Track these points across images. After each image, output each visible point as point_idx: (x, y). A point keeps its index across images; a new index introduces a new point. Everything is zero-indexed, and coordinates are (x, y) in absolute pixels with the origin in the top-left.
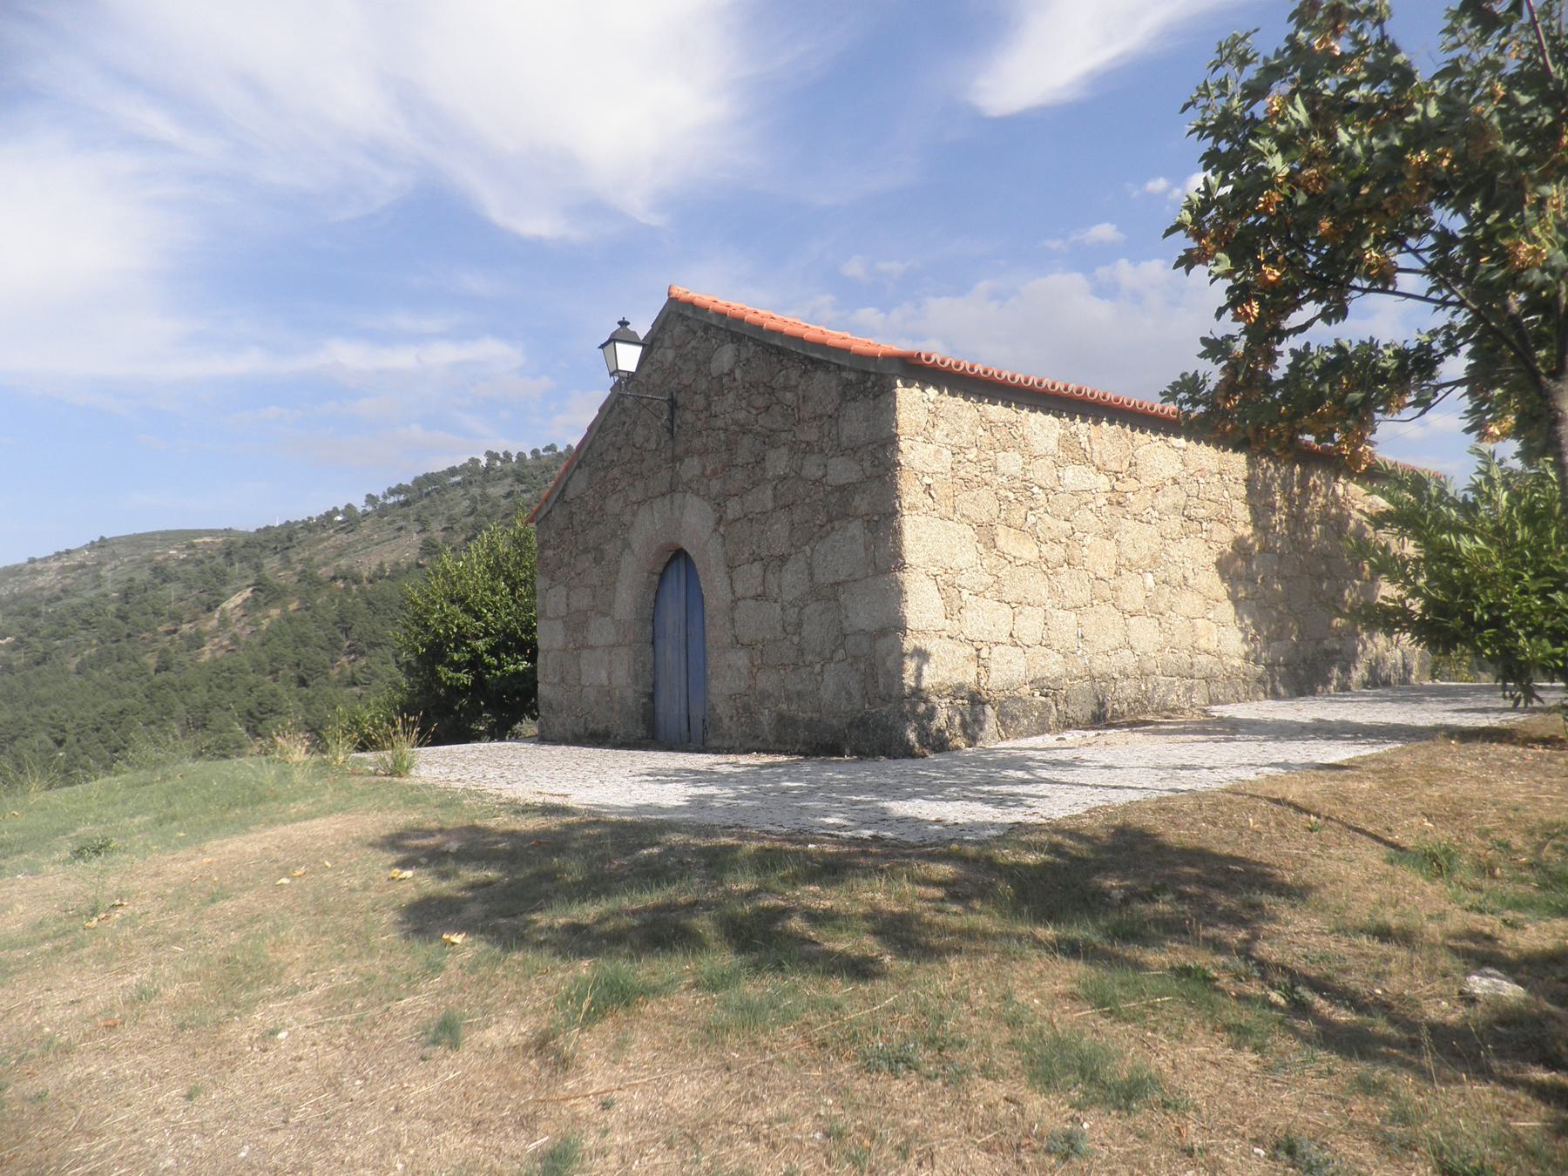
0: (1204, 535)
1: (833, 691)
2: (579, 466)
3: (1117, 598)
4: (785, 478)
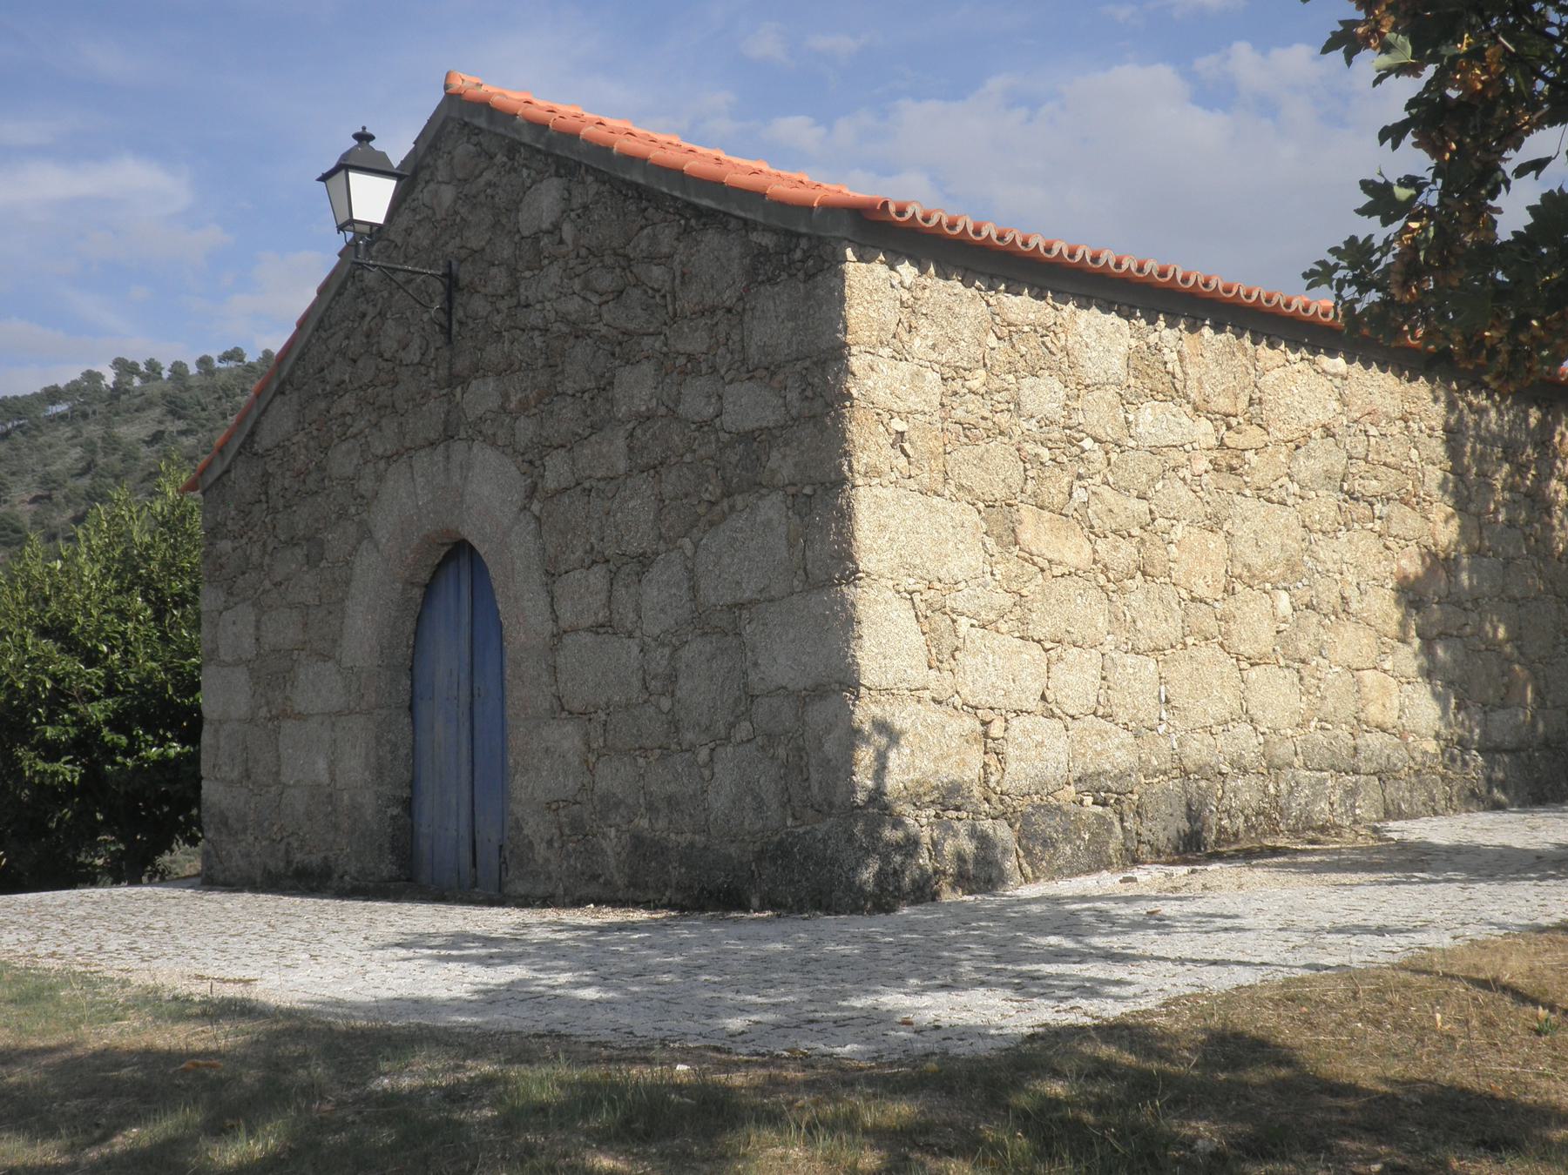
0: (1377, 525)
1: (731, 794)
2: (281, 391)
3: (1227, 634)
4: (647, 418)
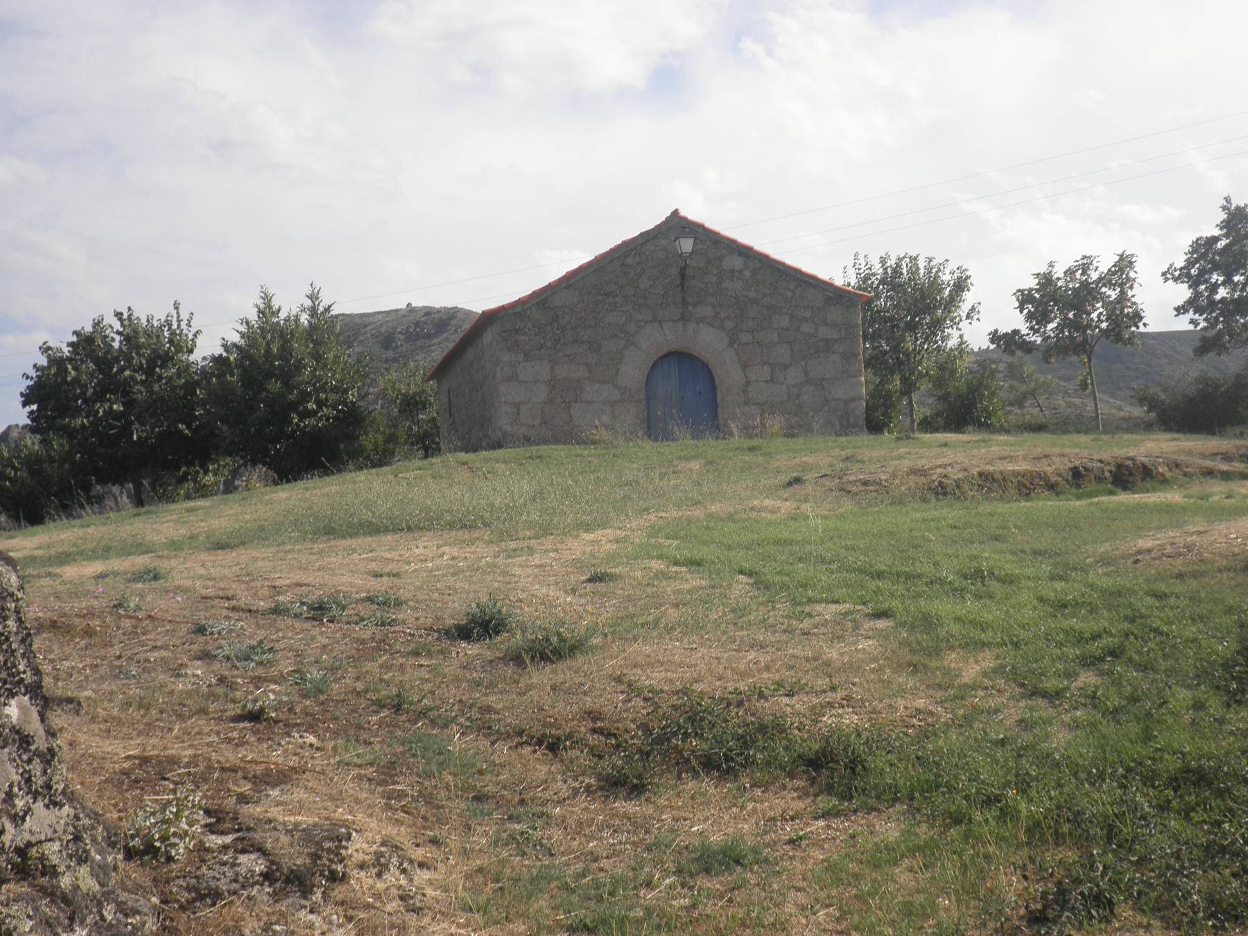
2: (567, 288)
4: (787, 330)
